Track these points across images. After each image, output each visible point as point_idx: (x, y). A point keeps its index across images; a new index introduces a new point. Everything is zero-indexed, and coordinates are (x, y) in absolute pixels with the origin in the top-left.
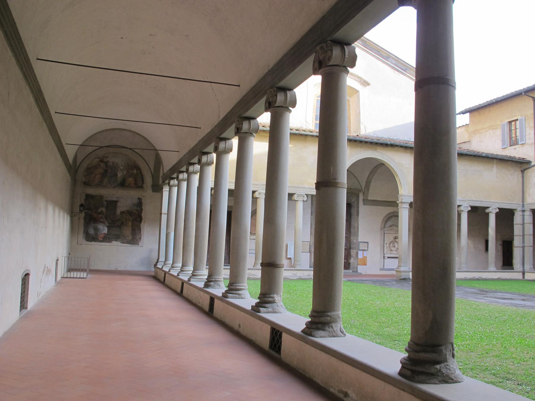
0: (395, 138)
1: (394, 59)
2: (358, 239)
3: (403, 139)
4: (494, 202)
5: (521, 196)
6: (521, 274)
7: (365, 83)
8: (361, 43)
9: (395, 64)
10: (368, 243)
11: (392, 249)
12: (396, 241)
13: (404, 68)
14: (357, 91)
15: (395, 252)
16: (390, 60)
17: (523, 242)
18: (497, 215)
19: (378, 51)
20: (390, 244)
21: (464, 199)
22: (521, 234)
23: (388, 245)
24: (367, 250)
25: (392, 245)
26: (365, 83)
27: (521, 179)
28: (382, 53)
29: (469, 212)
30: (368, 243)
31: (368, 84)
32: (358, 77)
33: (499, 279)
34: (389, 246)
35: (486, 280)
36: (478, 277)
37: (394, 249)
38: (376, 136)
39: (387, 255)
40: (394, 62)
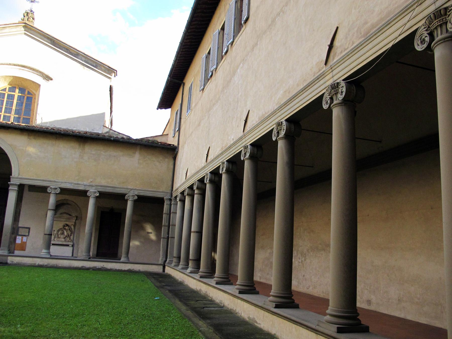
0: (75, 129)
1: (84, 56)
2: (18, 224)
3: (85, 130)
4: (131, 189)
5: (170, 183)
6: (162, 267)
7: (48, 78)
8: (50, 42)
9: (85, 61)
10: (29, 228)
11: (60, 236)
12: (65, 229)
13: (95, 65)
14: (39, 86)
15: (64, 240)
16: (80, 57)
17: (168, 234)
18: (135, 202)
19: (67, 49)
20: (58, 231)
21: (91, 184)
22: (167, 224)
23: (55, 232)
24: (28, 235)
25: (60, 232)
26: (48, 78)
27: (172, 167)
28: (71, 51)
29: (97, 197)
30: (29, 228)
31: (52, 79)
32: (40, 72)
33: (95, 269)
34: (57, 234)
35: (110, 270)
36: (100, 267)
37: (62, 236)
38: (53, 126)
39: (52, 242)
40: (83, 59)
